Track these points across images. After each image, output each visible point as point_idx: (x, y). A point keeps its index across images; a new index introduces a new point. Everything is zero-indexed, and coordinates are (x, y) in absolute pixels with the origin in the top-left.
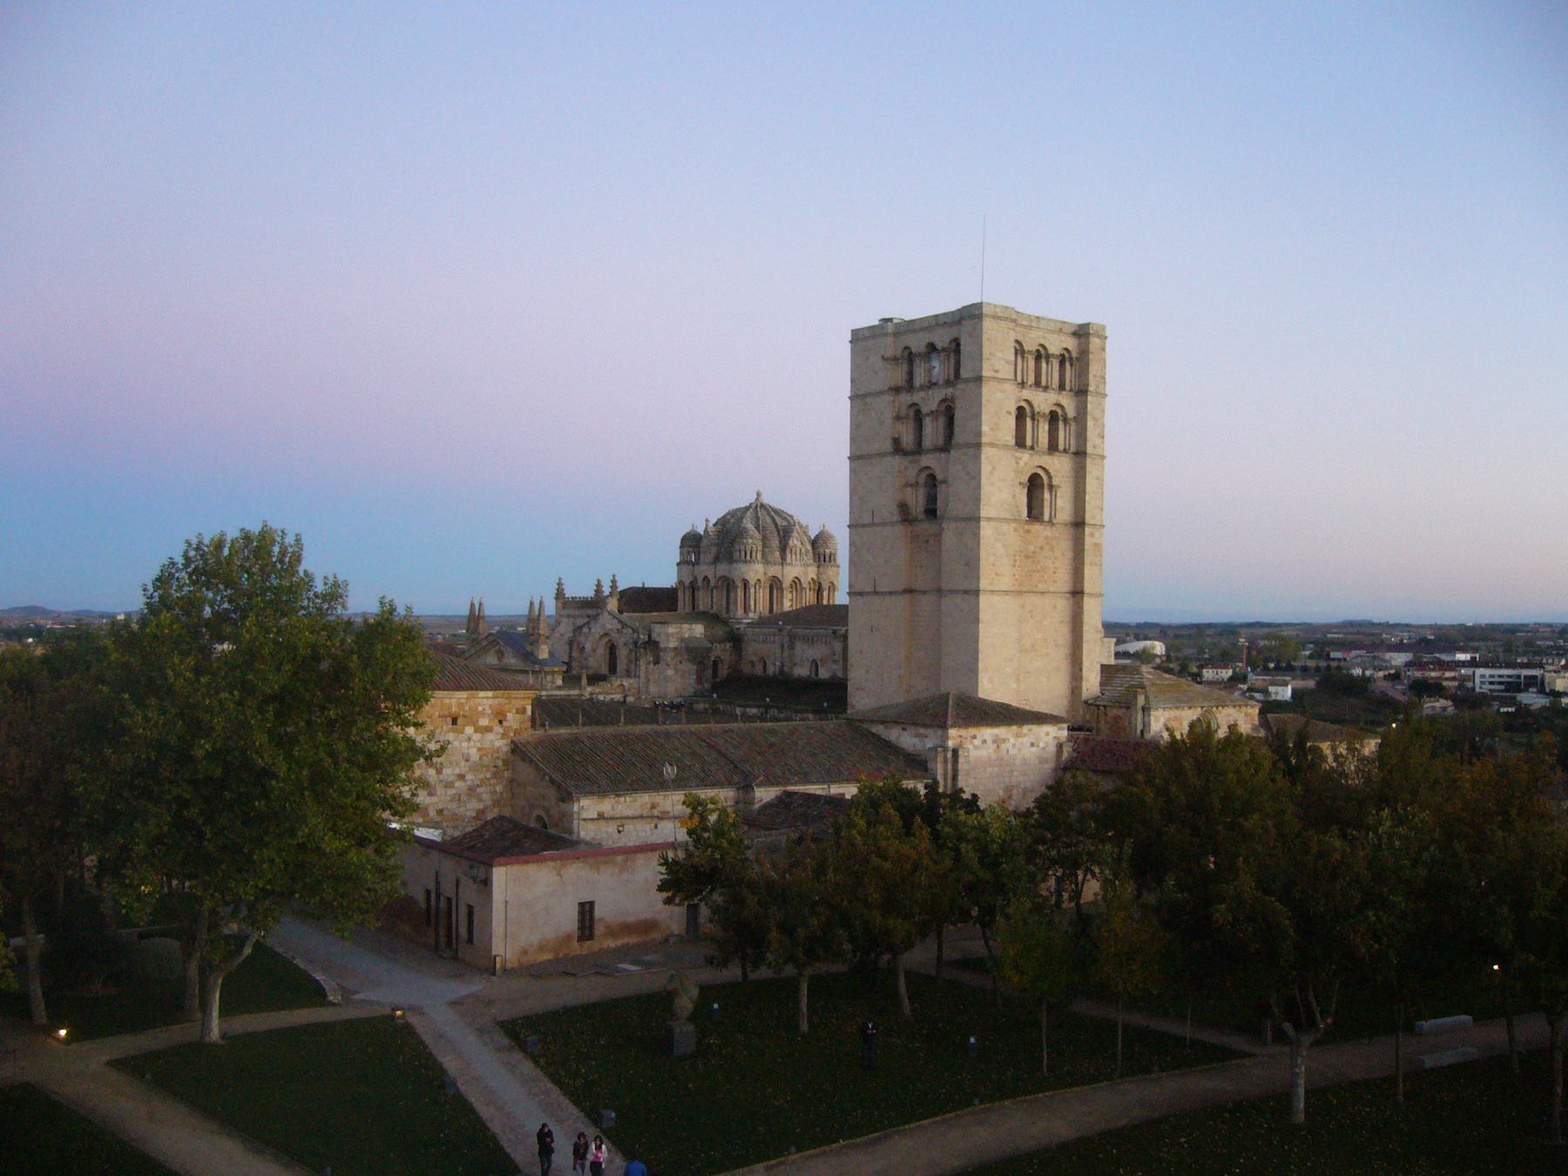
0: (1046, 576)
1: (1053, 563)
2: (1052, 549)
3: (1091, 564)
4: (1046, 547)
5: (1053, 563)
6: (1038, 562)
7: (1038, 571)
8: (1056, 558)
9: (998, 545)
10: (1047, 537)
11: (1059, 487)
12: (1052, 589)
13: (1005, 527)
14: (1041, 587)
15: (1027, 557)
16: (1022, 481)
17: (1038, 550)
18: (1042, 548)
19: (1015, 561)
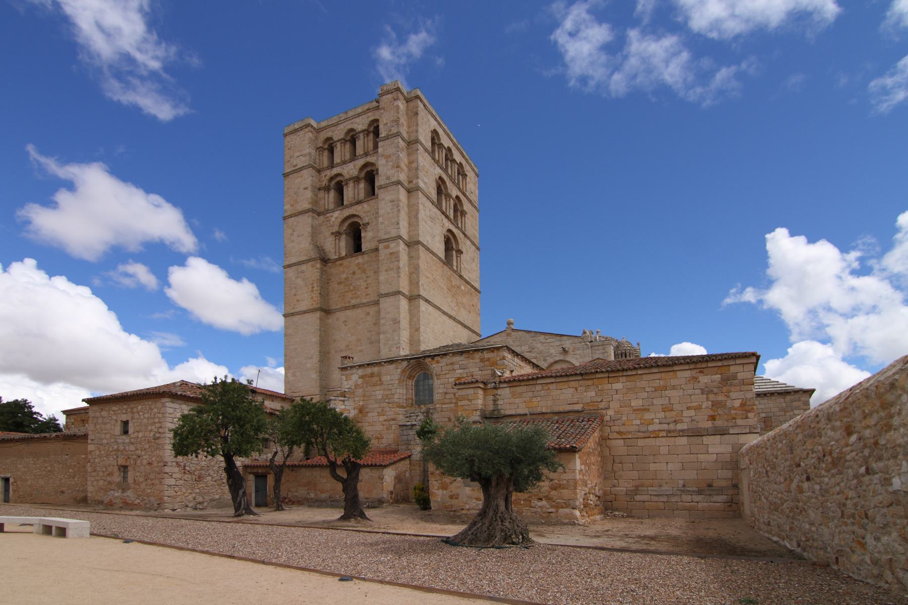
0: (359, 293)
1: (366, 281)
2: (364, 271)
3: (386, 271)
4: (357, 272)
5: (366, 281)
6: (351, 284)
7: (352, 290)
8: (367, 277)
9: (299, 281)
10: (358, 264)
11: (368, 223)
12: (364, 301)
13: (304, 267)
14: (353, 302)
15: (339, 283)
16: (334, 231)
17: (349, 276)
18: (354, 273)
19: (313, 287)
